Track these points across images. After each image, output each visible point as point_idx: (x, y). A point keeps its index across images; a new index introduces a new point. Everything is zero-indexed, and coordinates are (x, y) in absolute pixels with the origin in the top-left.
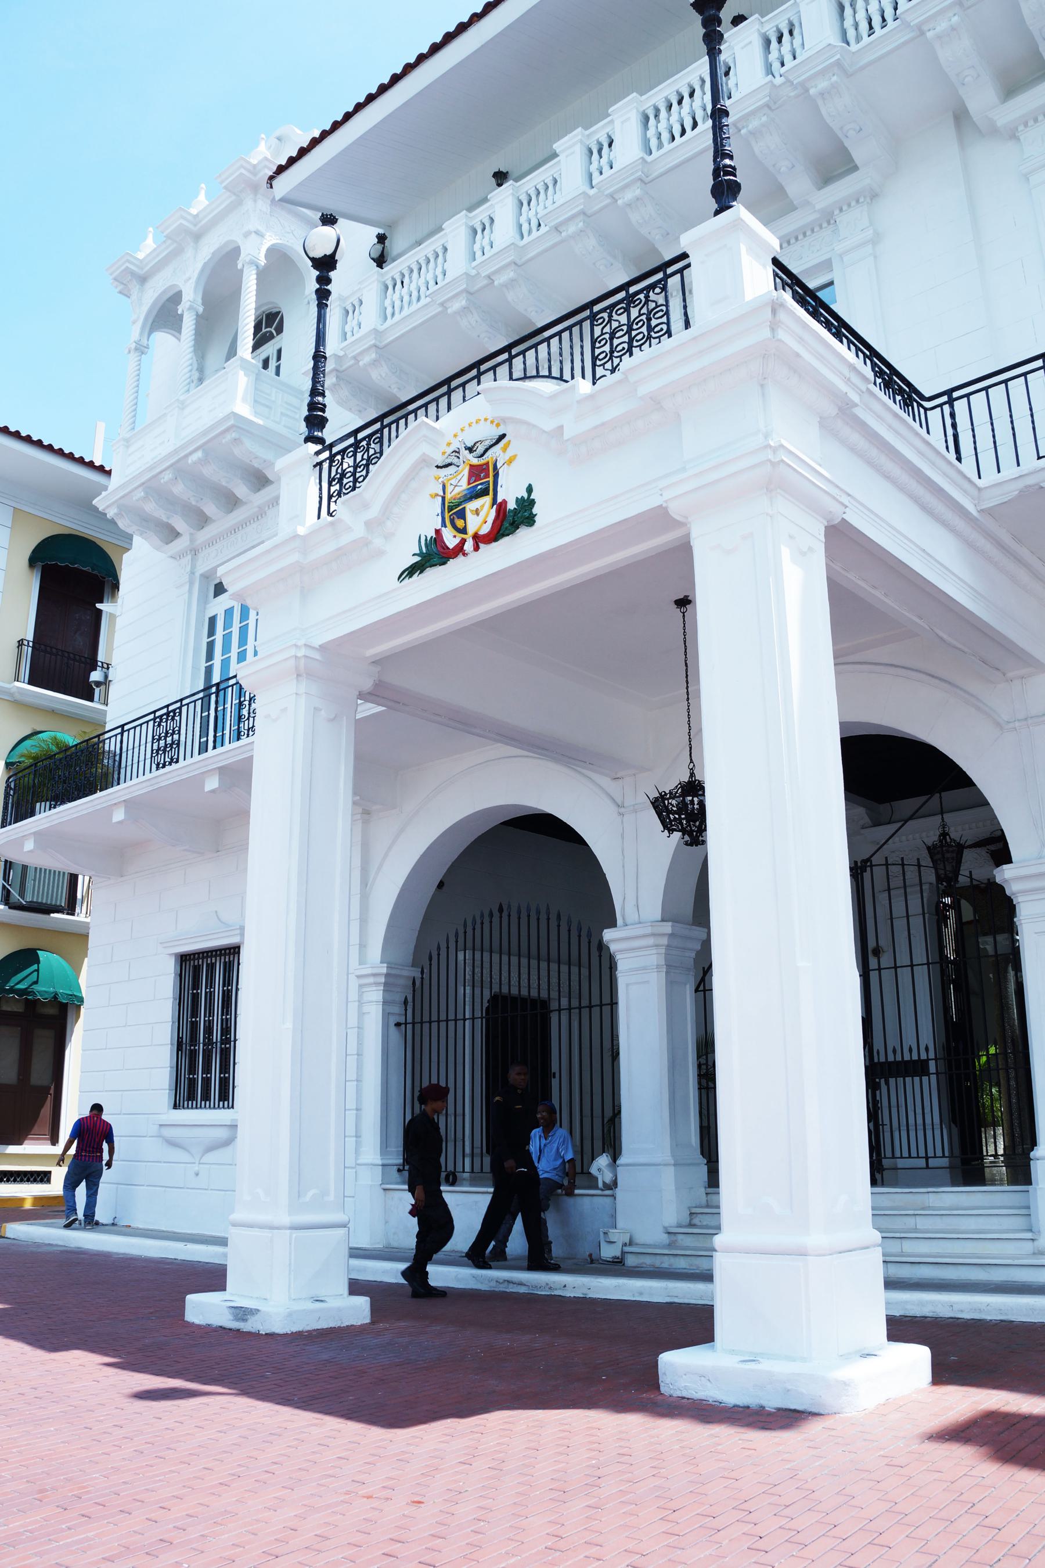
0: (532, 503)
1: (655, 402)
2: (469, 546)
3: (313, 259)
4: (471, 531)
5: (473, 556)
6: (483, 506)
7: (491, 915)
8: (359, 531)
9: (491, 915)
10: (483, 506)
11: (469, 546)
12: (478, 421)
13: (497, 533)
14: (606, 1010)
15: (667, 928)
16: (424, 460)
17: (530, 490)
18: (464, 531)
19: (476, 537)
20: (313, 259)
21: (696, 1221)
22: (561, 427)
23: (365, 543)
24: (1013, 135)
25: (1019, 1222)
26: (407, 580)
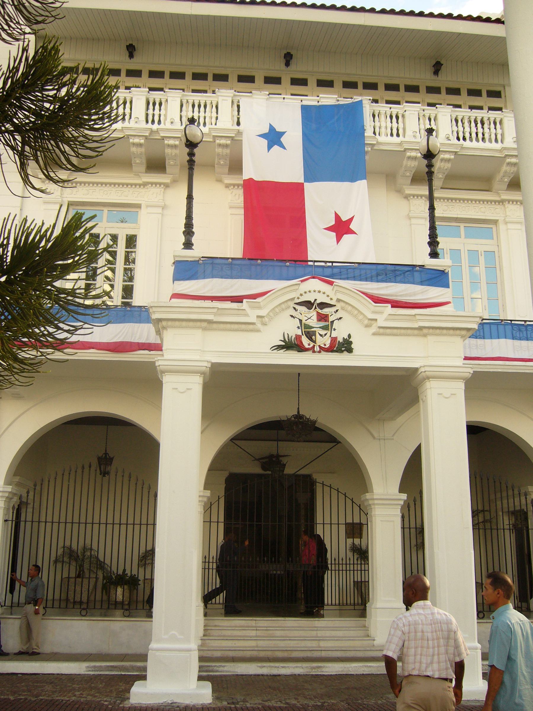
0: (351, 343)
1: (421, 328)
2: (317, 349)
3: (187, 140)
4: (318, 344)
5: (317, 355)
6: (326, 334)
7: (83, 468)
8: (252, 319)
9: (83, 468)
10: (326, 334)
11: (317, 349)
12: (319, 292)
13: (330, 350)
14: (150, 527)
15: (208, 493)
16: (293, 299)
17: (349, 336)
18: (315, 342)
19: (319, 346)
20: (187, 140)
21: (207, 633)
22: (376, 320)
23: (253, 324)
24: (407, 197)
25: (361, 633)
26: (275, 351)
